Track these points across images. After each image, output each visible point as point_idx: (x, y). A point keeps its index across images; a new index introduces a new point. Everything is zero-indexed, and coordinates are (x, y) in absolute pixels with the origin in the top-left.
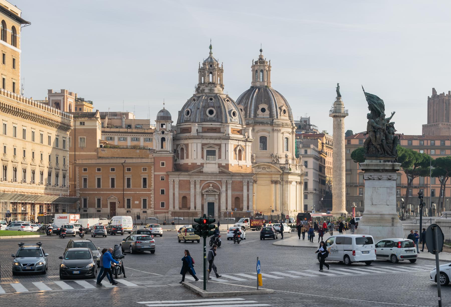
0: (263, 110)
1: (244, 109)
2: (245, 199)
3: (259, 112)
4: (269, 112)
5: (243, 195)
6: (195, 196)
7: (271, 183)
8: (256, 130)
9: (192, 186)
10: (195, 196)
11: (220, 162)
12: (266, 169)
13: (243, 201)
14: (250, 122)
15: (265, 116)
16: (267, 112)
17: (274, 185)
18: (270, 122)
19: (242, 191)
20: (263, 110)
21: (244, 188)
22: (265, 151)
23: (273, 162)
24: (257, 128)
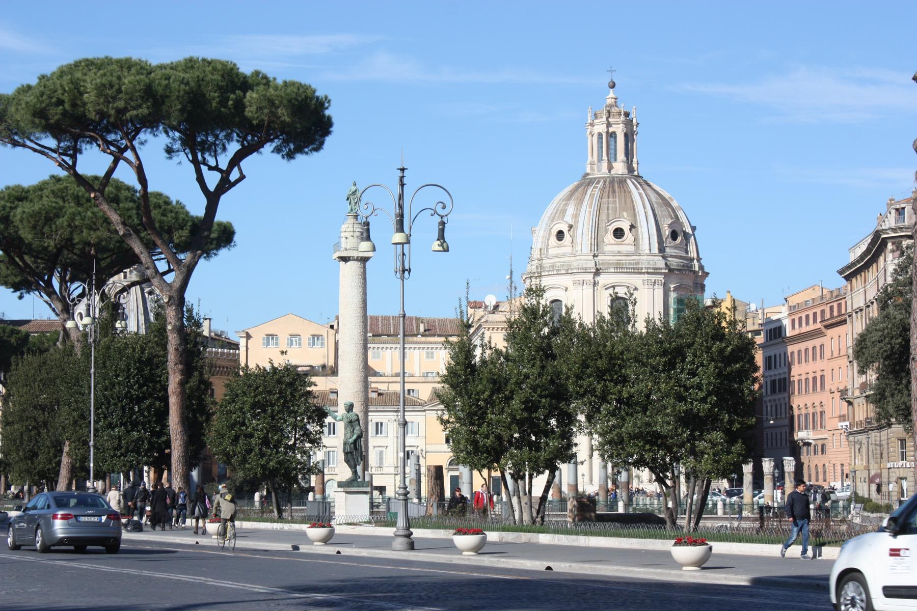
0: (618, 233)
20: (618, 233)
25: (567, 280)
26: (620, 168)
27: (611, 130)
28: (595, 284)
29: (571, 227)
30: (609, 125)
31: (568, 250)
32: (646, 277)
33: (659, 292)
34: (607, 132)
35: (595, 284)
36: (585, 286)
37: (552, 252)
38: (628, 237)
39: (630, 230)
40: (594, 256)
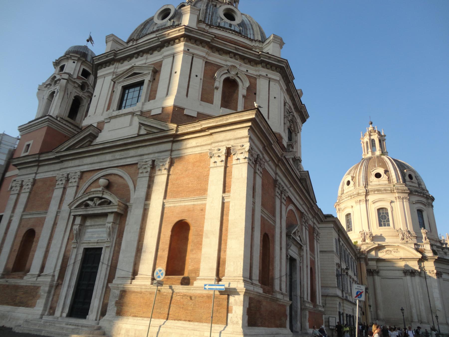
0: (378, 176)
1: (352, 180)
2: (211, 225)
3: (372, 178)
4: (387, 177)
5: (203, 210)
6: (55, 224)
7: (403, 275)
8: (370, 202)
9: (57, 193)
10: (55, 224)
11: (146, 108)
12: (393, 252)
13: (200, 235)
14: (360, 191)
15: (381, 182)
16: (384, 177)
17: (408, 278)
18: (389, 189)
19: (202, 191)
20: (378, 176)
21: (211, 178)
22: (387, 227)
23: (403, 241)
24: (371, 198)
25: (352, 202)
26: (378, 153)
27: (372, 137)
28: (366, 201)
29: (353, 178)
30: (370, 135)
31: (353, 188)
32: (397, 195)
33: (406, 204)
34: (370, 139)
35: (366, 201)
36: (361, 203)
37: (345, 192)
38: (384, 177)
39: (385, 173)
40: (365, 187)
